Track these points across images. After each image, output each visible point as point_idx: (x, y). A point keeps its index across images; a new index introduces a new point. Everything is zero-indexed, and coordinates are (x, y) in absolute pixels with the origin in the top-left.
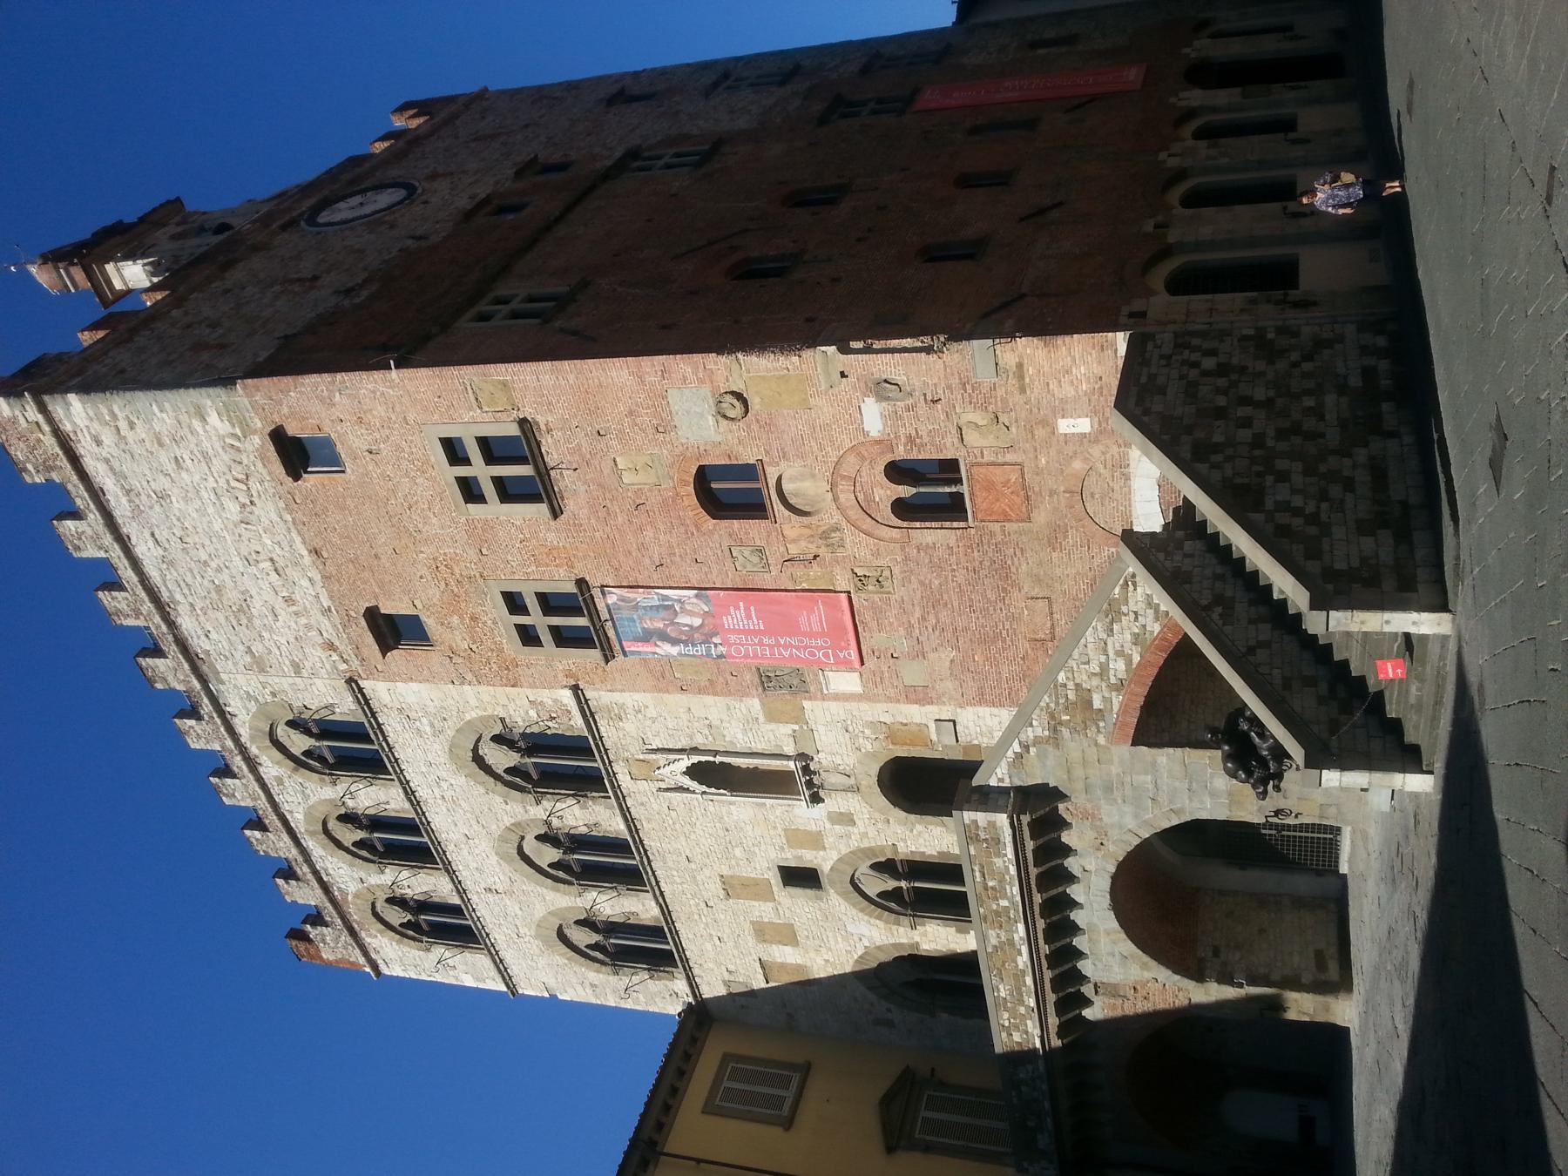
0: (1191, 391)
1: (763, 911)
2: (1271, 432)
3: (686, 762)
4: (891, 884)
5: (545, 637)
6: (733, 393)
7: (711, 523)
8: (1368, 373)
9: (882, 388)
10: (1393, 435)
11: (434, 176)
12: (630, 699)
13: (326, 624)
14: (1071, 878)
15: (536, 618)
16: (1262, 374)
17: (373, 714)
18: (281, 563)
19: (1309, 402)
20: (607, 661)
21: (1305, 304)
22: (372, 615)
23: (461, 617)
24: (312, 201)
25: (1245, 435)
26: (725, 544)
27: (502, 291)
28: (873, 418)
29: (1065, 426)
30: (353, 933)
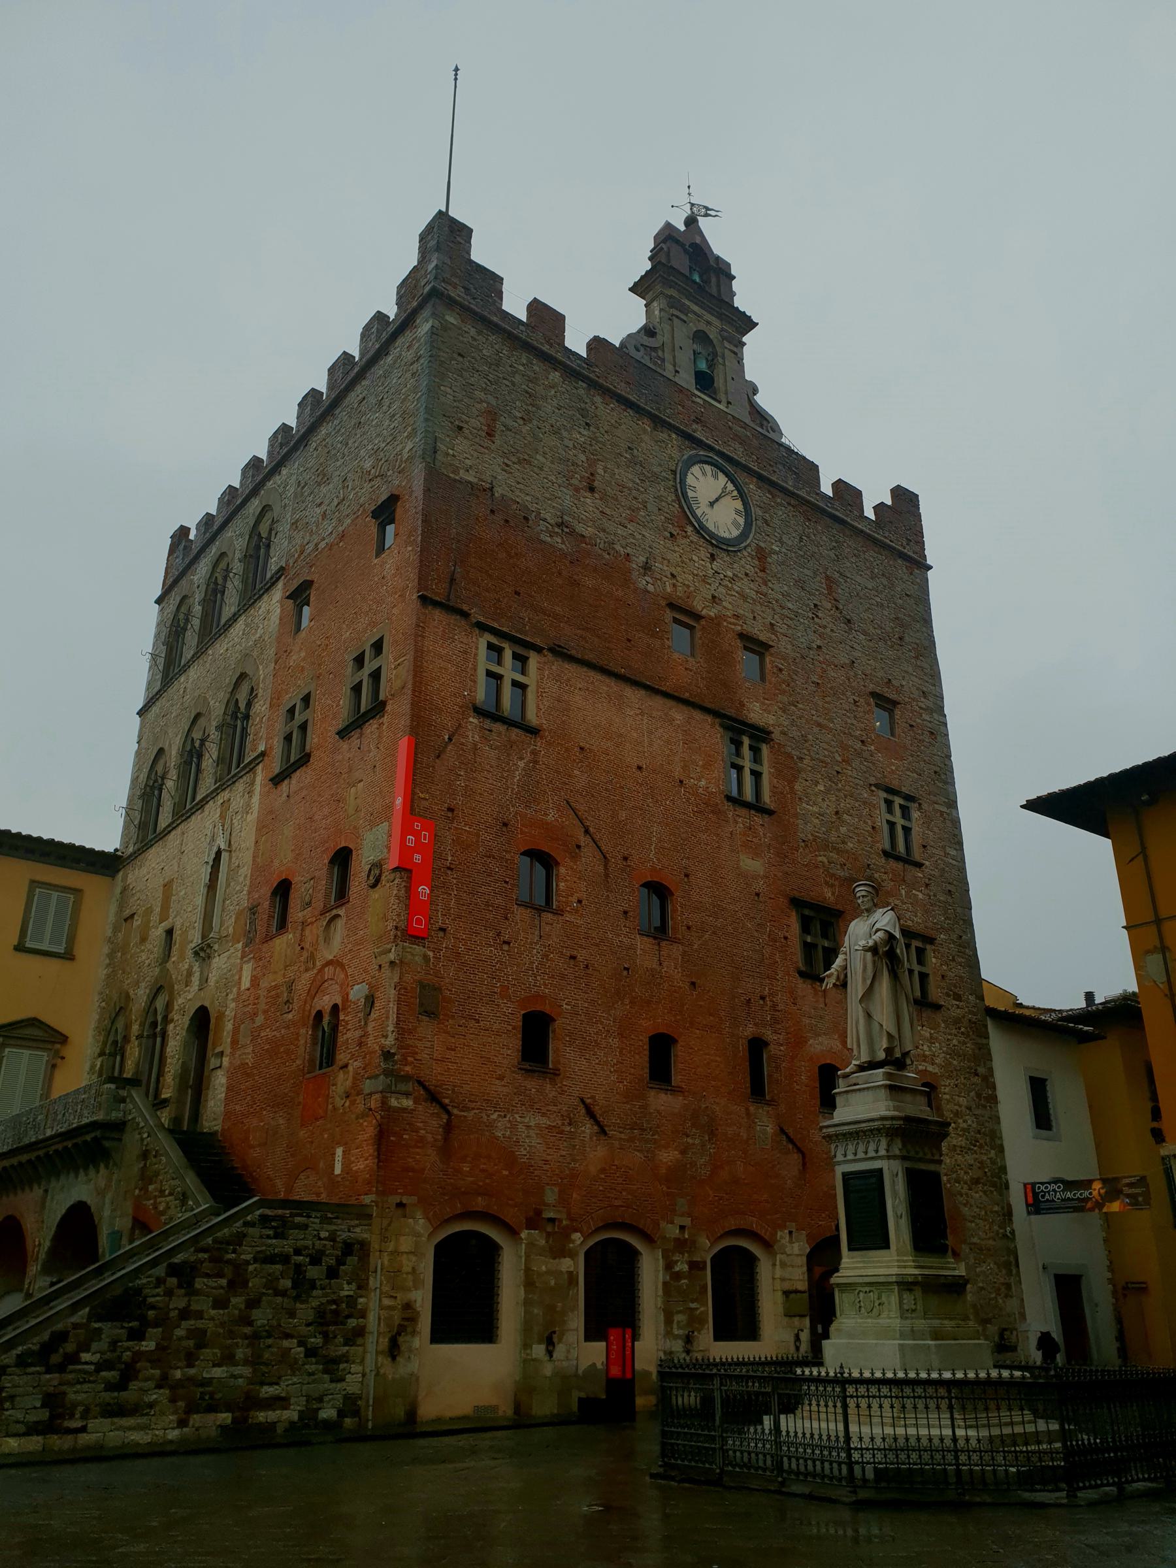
0: (271, 1259)
1: (155, 917)
2: (200, 1324)
3: (222, 847)
4: (159, 1018)
5: (288, 729)
6: (380, 876)
7: (326, 861)
8: (281, 1402)
9: (370, 1000)
10: (182, 1423)
11: (761, 555)
12: (256, 800)
13: (311, 546)
14: (86, 1169)
15: (299, 718)
16: (292, 1314)
17: (267, 590)
18: (341, 507)
19: (240, 1354)
20: (271, 780)
21: (393, 1350)
22: (307, 585)
23: (304, 659)
24: (738, 453)
25: (201, 1304)
26: (317, 874)
27: (534, 661)
28: (358, 992)
29: (339, 1151)
30: (176, 582)
